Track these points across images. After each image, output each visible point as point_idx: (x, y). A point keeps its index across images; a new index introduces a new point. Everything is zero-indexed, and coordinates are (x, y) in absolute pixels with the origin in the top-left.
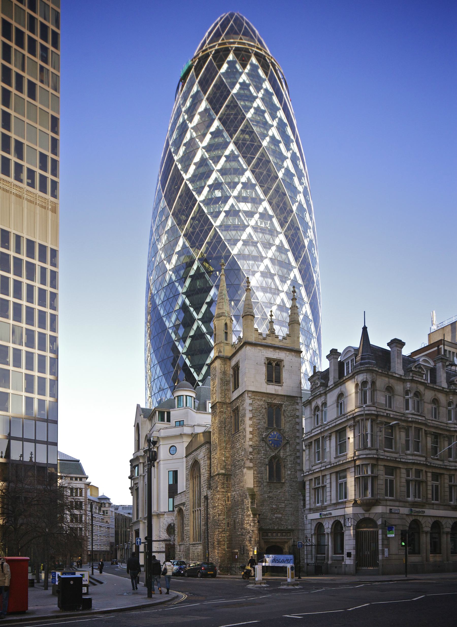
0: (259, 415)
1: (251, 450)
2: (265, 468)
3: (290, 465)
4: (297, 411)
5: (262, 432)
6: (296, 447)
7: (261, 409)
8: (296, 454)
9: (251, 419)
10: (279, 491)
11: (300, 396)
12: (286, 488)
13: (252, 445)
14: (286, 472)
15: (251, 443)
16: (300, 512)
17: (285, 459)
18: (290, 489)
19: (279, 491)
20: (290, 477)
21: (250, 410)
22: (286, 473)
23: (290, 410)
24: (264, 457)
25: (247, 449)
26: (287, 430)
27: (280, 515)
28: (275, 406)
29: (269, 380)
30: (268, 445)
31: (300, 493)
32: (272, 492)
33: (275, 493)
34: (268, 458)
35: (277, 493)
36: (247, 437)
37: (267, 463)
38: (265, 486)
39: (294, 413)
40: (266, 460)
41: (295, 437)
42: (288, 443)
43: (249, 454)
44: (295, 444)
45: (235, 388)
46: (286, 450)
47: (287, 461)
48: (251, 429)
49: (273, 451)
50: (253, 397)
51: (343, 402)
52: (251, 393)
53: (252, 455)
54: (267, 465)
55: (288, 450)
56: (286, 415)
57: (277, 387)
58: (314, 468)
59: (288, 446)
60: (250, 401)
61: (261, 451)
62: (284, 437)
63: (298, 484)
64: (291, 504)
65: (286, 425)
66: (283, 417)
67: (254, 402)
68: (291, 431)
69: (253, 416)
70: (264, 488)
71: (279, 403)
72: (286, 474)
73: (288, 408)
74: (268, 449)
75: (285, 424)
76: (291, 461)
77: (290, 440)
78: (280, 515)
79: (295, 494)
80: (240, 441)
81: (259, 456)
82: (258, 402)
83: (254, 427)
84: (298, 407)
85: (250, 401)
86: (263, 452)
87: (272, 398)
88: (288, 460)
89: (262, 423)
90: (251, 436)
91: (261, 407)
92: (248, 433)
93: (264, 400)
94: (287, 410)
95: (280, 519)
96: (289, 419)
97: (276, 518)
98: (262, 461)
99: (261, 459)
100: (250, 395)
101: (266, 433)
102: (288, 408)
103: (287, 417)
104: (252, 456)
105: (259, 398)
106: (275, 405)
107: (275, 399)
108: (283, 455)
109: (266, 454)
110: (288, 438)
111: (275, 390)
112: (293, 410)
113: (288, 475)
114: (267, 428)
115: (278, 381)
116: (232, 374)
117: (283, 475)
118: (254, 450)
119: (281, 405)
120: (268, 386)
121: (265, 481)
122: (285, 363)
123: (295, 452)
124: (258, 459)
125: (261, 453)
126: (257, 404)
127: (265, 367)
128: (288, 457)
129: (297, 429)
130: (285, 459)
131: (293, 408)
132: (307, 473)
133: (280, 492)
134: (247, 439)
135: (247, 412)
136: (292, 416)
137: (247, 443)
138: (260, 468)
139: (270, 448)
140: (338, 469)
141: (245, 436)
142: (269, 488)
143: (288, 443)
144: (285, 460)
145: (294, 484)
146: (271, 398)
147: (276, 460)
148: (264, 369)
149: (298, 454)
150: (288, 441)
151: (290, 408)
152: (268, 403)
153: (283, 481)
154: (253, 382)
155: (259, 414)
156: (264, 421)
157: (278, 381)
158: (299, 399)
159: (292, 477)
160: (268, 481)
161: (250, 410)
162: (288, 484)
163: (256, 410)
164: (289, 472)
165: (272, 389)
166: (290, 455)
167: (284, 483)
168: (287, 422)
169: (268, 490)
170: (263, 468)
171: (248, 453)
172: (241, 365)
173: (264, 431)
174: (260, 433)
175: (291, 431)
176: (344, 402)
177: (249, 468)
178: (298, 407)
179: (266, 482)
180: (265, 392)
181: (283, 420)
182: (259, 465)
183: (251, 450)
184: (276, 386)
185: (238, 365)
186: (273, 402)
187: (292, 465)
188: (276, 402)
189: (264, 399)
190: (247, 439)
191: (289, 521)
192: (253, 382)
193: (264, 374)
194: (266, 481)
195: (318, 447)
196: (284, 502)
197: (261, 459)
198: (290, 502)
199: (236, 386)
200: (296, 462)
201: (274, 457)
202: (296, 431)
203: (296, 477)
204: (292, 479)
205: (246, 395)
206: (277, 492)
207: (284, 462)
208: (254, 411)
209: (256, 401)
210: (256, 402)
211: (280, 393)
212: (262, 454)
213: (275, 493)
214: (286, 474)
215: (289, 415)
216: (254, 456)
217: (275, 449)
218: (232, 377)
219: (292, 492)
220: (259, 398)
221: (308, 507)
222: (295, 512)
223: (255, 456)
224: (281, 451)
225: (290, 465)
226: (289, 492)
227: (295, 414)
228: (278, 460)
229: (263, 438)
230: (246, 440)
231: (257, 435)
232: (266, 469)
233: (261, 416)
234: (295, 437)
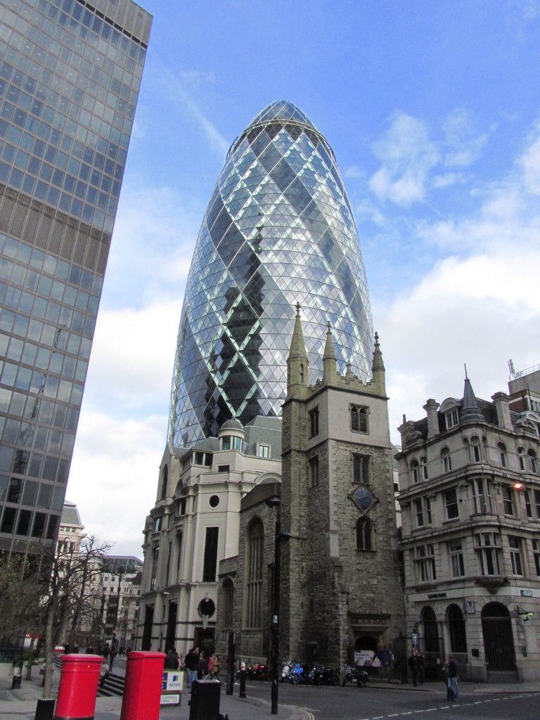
10: (370, 563)
12: (379, 558)
15: (335, 501)
22: (377, 540)
27: (372, 595)
28: (361, 457)
29: (355, 427)
30: (355, 503)
42: (378, 502)
48: (335, 484)
49: (361, 512)
54: (354, 528)
55: (378, 510)
58: (415, 534)
59: (378, 505)
62: (374, 495)
63: (392, 554)
65: (374, 481)
74: (355, 508)
78: (372, 595)
84: (387, 459)
90: (335, 492)
95: (373, 600)
97: (368, 598)
106: (362, 456)
107: (361, 449)
115: (364, 429)
118: (339, 508)
122: (371, 410)
132: (407, 541)
139: (358, 508)
140: (448, 538)
141: (327, 492)
143: (378, 502)
146: (356, 448)
147: (366, 522)
148: (348, 415)
149: (390, 516)
152: (354, 454)
153: (375, 550)
157: (364, 429)
164: (381, 539)
165: (358, 437)
167: (375, 552)
177: (334, 532)
178: (387, 459)
180: (350, 441)
181: (372, 475)
188: (363, 452)
191: (384, 604)
195: (419, 508)
203: (389, 545)
204: (385, 548)
211: (366, 443)
217: (364, 508)
221: (408, 584)
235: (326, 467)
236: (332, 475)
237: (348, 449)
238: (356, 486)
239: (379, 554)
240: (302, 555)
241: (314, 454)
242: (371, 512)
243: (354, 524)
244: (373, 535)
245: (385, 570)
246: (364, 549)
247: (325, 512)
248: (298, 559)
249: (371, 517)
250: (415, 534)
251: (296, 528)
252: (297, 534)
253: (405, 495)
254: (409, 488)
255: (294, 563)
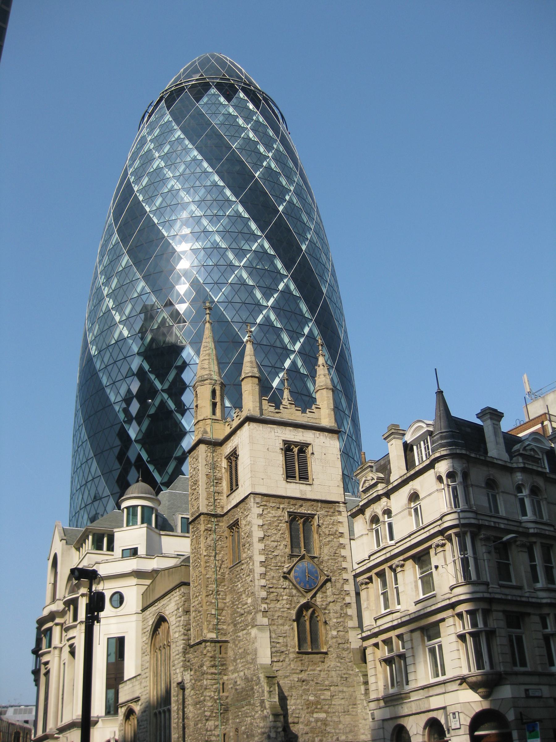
0: (276, 534)
1: (264, 594)
2: (290, 626)
3: (335, 620)
4: (341, 525)
5: (282, 563)
6: (343, 587)
7: (279, 523)
8: (344, 599)
9: (261, 540)
10: (318, 669)
11: (343, 500)
13: (265, 586)
14: (329, 633)
15: (263, 582)
16: (360, 706)
17: (325, 609)
18: (339, 664)
19: (318, 669)
20: (337, 641)
21: (258, 526)
23: (329, 525)
24: (288, 606)
25: (257, 593)
26: (326, 558)
30: (294, 585)
31: (357, 670)
32: (306, 670)
33: (311, 673)
34: (294, 607)
35: (316, 672)
36: (256, 571)
37: (294, 618)
38: (293, 660)
39: (335, 528)
40: (292, 612)
41: (340, 569)
43: (260, 602)
44: (341, 581)
45: (232, 489)
46: (325, 592)
47: (329, 613)
48: (263, 558)
49: (304, 596)
50: (264, 503)
51: (418, 506)
52: (260, 496)
53: (266, 603)
55: (329, 592)
56: (321, 533)
57: (303, 487)
59: (329, 585)
60: (260, 511)
61: (282, 596)
63: (351, 655)
64: (343, 692)
66: (316, 536)
67: (265, 512)
68: (332, 559)
69: (265, 535)
70: (290, 664)
71: (309, 512)
72: (330, 636)
73: (324, 521)
74: (294, 591)
75: (320, 548)
76: (336, 613)
77: (331, 574)
79: (347, 674)
80: (244, 580)
81: (278, 605)
82: (273, 512)
83: (267, 554)
84: (340, 518)
85: (260, 511)
86: (285, 597)
87: (296, 505)
88: (331, 611)
89: (282, 547)
91: (278, 520)
92: (257, 564)
93: (283, 509)
94: (322, 524)
96: (328, 539)
98: (285, 615)
99: (282, 610)
100: (258, 500)
101: (289, 563)
102: (324, 521)
103: (323, 535)
104: (265, 606)
105: (273, 505)
106: (302, 516)
107: (301, 506)
108: (322, 601)
109: (291, 601)
110: (327, 571)
111: (301, 491)
112: (333, 524)
113: (333, 638)
114: (290, 555)
116: (226, 467)
117: (324, 638)
118: (269, 593)
119: (313, 516)
120: (289, 484)
121: (292, 650)
123: (342, 596)
124: (276, 611)
125: (282, 600)
126: (270, 515)
127: (281, 455)
128: (331, 604)
129: (343, 556)
130: (325, 609)
131: (332, 521)
133: (320, 671)
134: (257, 576)
135: (255, 528)
136: (331, 535)
137: (257, 582)
138: (281, 627)
139: (298, 590)
142: (299, 663)
143: (328, 580)
144: (327, 611)
145: (345, 654)
150: (328, 576)
151: (328, 520)
153: (324, 650)
154: (263, 479)
155: (275, 532)
156: (284, 543)
158: (341, 505)
159: (340, 641)
160: (297, 650)
161: (258, 526)
162: (335, 655)
163: (270, 524)
164: (334, 633)
166: (334, 601)
167: (326, 653)
168: (326, 544)
169: (298, 666)
170: (286, 627)
171: (260, 600)
172: (240, 452)
173: (285, 561)
174: (279, 564)
175: (332, 559)
176: (420, 506)
179: (294, 652)
182: (281, 622)
183: (264, 594)
184: (301, 485)
185: (236, 454)
186: (299, 511)
187: (339, 620)
188: (303, 510)
189: (282, 506)
190: (256, 575)
192: (263, 479)
193: (281, 466)
194: (293, 650)
196: (329, 690)
197: (282, 610)
198: (340, 688)
199: (234, 485)
200: (346, 614)
201: (306, 606)
202: (341, 559)
203: (347, 642)
205: (252, 500)
206: (314, 670)
207: (325, 614)
208: (266, 527)
209: (269, 510)
210: (269, 512)
212: (284, 602)
213: (311, 673)
214: (330, 636)
215: (327, 533)
216: (269, 606)
217: (308, 591)
218: (226, 471)
219: (342, 669)
220: (273, 505)
222: (350, 707)
223: (272, 605)
224: (318, 595)
225: (335, 620)
226: (338, 668)
227: (337, 531)
228: (313, 612)
229: (284, 573)
230: (254, 576)
231: (274, 568)
232: (293, 628)
233: (279, 535)
234: (340, 569)
235: (250, 535)
236: (258, 546)
237: (282, 506)
238: (296, 560)
239: (332, 656)
240: (222, 665)
241: (234, 516)
242: (319, 595)
243: (293, 613)
244: (322, 629)
245: (342, 677)
246: (310, 650)
247: (249, 601)
248: (216, 671)
249: (318, 603)
250: (380, 622)
251: (211, 626)
252: (212, 636)
253: (364, 568)
254: (370, 557)
255: (210, 677)
